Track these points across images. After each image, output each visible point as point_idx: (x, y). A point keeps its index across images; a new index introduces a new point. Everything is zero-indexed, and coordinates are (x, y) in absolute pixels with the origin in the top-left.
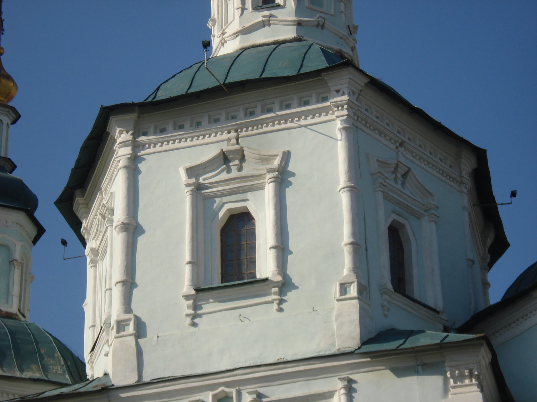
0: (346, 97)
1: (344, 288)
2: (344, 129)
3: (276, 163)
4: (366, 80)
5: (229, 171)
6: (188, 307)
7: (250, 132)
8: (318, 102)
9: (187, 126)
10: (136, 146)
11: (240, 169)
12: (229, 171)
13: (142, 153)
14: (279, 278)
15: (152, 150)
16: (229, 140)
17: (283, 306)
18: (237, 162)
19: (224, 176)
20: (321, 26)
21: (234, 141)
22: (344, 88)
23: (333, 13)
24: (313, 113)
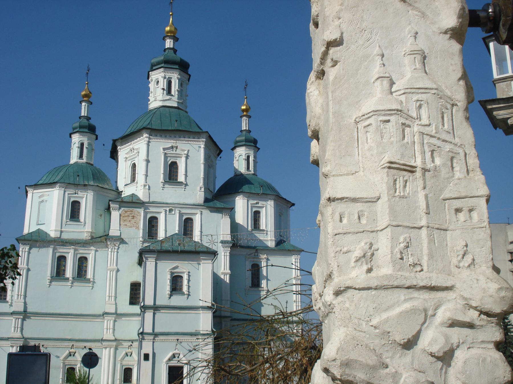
0: (205, 140)
1: (201, 188)
2: (204, 148)
3: (186, 152)
4: (208, 135)
5: (173, 151)
6: (162, 185)
8: (197, 139)
10: (150, 138)
11: (176, 151)
12: (173, 151)
13: (150, 140)
14: (186, 183)
15: (153, 140)
17: (185, 189)
18: (175, 149)
19: (172, 152)
20: (182, 103)
21: (175, 143)
24: (196, 141)
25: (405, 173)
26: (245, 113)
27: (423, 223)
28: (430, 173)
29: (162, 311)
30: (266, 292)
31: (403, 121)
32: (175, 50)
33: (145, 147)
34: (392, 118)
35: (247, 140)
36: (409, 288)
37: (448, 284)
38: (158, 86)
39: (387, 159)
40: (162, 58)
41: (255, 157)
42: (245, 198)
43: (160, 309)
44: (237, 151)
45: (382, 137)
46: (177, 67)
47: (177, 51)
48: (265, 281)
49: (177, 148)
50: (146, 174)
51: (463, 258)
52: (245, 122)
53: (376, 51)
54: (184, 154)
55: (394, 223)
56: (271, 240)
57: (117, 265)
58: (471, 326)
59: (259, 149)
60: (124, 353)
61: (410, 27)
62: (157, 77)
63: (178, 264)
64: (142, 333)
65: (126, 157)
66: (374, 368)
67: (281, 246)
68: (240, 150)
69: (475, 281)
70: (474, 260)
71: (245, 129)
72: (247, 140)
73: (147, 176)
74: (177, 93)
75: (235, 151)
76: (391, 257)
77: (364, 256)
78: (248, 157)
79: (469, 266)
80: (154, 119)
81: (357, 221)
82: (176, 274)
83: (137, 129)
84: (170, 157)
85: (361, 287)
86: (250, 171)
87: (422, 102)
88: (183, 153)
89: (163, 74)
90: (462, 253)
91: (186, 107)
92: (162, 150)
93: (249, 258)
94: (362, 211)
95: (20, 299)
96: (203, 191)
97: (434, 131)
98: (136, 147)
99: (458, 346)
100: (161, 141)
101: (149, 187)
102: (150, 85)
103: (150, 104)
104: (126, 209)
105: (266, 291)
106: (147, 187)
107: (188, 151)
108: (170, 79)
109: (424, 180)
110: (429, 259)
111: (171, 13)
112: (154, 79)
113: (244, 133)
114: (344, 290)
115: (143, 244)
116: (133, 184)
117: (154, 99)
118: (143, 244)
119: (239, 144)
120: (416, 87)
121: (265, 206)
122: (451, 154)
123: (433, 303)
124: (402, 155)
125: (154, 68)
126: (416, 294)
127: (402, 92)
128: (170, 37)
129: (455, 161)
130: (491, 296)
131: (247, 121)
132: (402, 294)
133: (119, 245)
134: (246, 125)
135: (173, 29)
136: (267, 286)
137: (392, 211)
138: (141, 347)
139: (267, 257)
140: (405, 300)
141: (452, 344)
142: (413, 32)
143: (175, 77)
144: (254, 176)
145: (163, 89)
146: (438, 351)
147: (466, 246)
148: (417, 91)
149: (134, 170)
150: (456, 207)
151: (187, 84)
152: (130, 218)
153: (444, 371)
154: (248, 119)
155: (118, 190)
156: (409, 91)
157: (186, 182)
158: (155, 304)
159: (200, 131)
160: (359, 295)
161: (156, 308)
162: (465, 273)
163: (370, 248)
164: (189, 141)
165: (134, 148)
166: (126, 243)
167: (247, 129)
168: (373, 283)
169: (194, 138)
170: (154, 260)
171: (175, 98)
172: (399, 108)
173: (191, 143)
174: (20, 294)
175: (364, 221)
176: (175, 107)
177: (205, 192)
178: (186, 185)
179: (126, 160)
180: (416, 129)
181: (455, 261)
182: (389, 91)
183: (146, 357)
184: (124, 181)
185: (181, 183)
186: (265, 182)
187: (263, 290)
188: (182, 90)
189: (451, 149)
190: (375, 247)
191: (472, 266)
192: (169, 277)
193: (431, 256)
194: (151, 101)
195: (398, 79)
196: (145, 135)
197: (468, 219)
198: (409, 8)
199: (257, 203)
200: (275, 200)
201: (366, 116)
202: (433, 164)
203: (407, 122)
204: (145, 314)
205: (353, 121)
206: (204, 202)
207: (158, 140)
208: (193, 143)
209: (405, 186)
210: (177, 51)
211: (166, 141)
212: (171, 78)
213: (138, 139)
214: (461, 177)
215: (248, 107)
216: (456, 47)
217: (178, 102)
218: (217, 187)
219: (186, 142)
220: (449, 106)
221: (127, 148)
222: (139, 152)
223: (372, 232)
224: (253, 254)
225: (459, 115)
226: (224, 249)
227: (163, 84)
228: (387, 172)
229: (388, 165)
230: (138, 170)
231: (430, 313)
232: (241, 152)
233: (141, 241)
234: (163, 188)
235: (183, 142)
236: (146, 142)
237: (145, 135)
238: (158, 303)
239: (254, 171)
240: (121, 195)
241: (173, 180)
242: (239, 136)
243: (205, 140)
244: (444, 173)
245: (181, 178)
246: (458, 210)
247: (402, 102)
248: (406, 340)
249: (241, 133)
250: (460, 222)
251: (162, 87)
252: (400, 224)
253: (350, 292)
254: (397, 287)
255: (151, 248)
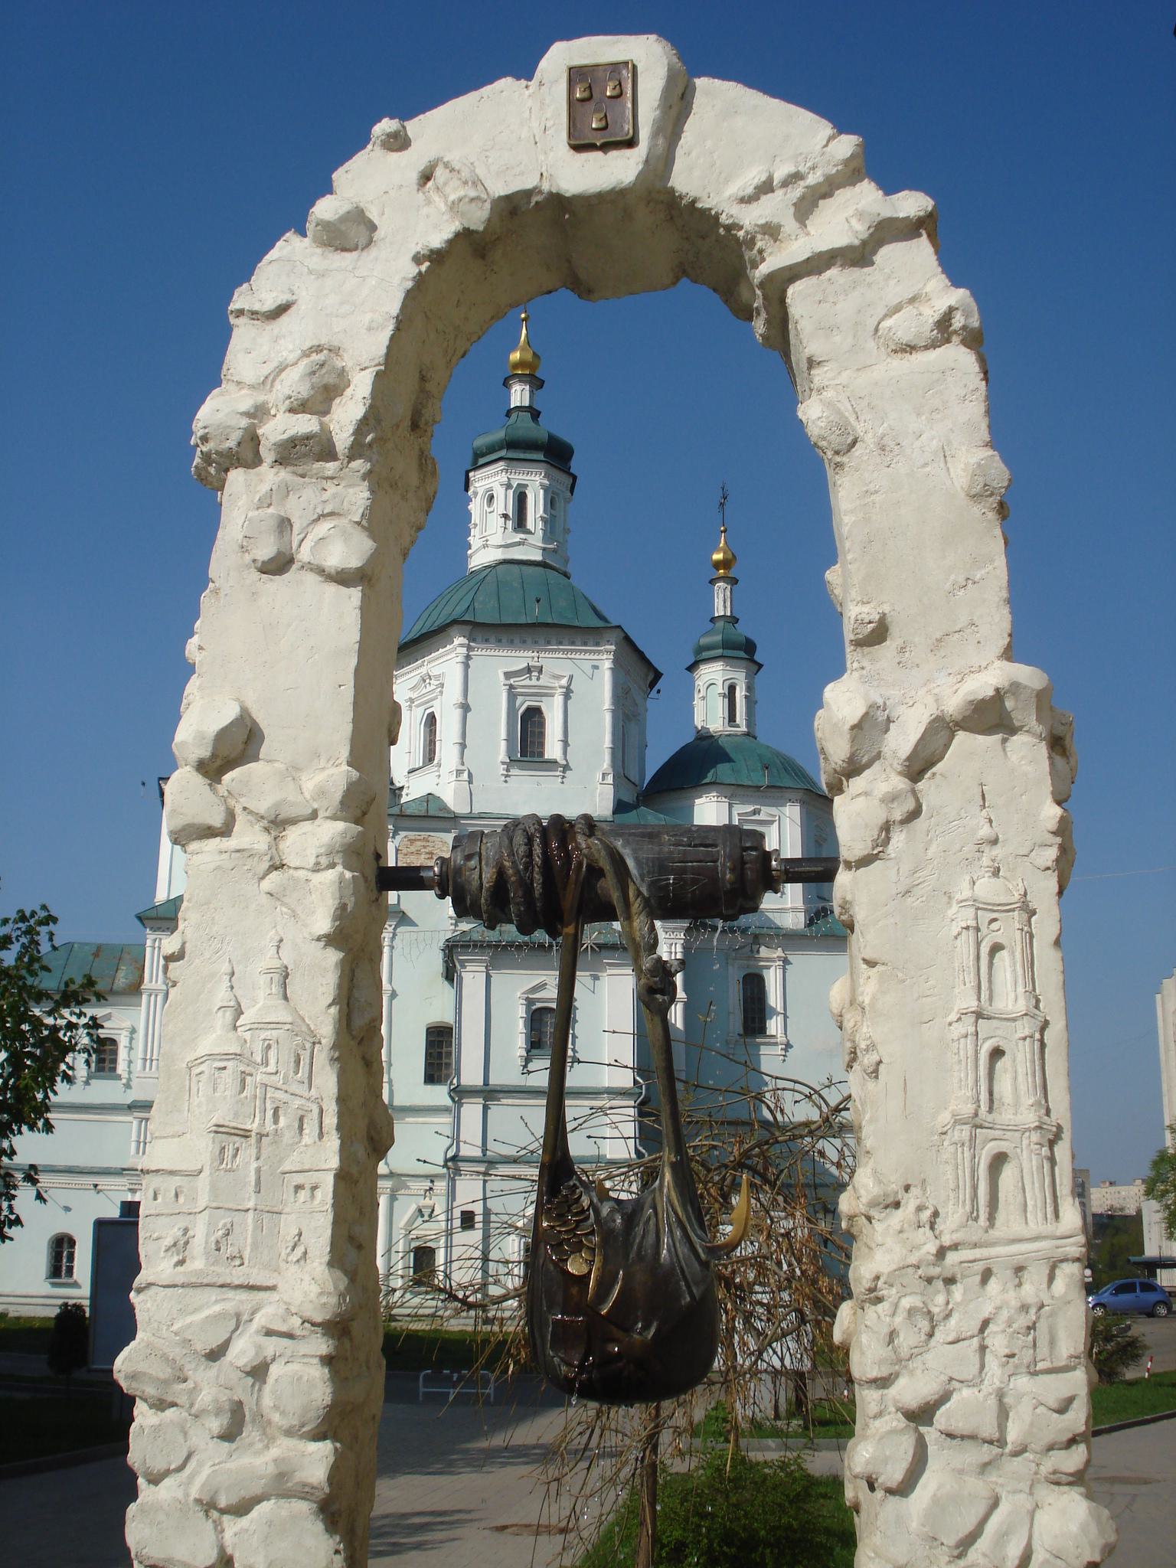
0: (613, 647)
3: (564, 682)
4: (623, 635)
5: (531, 679)
7: (546, 655)
8: (594, 646)
9: (504, 640)
10: (469, 648)
11: (538, 679)
12: (531, 679)
14: (564, 763)
15: (479, 653)
16: (533, 658)
18: (536, 674)
19: (527, 682)
20: (555, 551)
21: (536, 659)
22: (613, 639)
23: (561, 541)
24: (590, 652)
25: (237, 1138)
26: (722, 571)
27: (251, 1204)
28: (268, 1138)
29: (504, 1101)
30: (782, 1049)
31: (242, 1068)
32: (534, 413)
33: (458, 670)
34: (230, 1064)
35: (727, 644)
36: (222, 1286)
37: (270, 1283)
38: (491, 509)
39: (214, 1121)
40: (500, 435)
41: (749, 688)
42: (724, 799)
43: (501, 1095)
44: (702, 672)
45: (215, 1090)
46: (540, 456)
47: (539, 413)
48: (779, 1018)
49: (540, 670)
50: (461, 741)
51: (293, 1250)
52: (721, 596)
53: (225, 968)
54: (561, 687)
55: (214, 1205)
56: (794, 909)
57: (391, 983)
58: (290, 1336)
59: (760, 666)
60: (414, 1207)
61: (274, 931)
62: (487, 487)
63: (544, 978)
64: (455, 1158)
65: (410, 698)
66: (166, 1383)
67: (822, 926)
68: (710, 670)
69: (299, 1281)
70: (305, 1253)
71: (722, 614)
72: (727, 644)
73: (463, 746)
74: (540, 525)
75: (696, 675)
76: (205, 1248)
77: (175, 1245)
78: (732, 689)
79: (298, 1261)
80: (480, 598)
81: (174, 1199)
82: (539, 1005)
83: (436, 624)
84: (522, 694)
85: (164, 1284)
86: (738, 726)
87: (271, 1042)
88: (557, 685)
89: (503, 477)
90: (291, 1244)
91: (567, 561)
92: (502, 677)
93: (735, 959)
94: (180, 1187)
95: (151, 1069)
96: (611, 782)
97: (281, 1082)
98: (434, 672)
99: (273, 1360)
100: (501, 653)
101: (470, 775)
102: (471, 506)
103: (471, 556)
104: (412, 835)
105: (784, 1046)
106: (465, 776)
107: (571, 678)
108: (522, 490)
109: (259, 1149)
110: (252, 1251)
111: (523, 316)
112: (481, 492)
113: (720, 624)
114: (145, 1287)
115: (456, 925)
116: (431, 768)
117: (480, 543)
118: (456, 925)
119: (706, 654)
120: (264, 1021)
121: (777, 818)
122: (301, 1113)
123: (250, 1306)
124: (236, 1115)
125: (481, 461)
126: (231, 1294)
127: (248, 1027)
128: (521, 379)
129: (306, 1120)
130: (311, 1302)
131: (728, 593)
132: (214, 1294)
133: (395, 929)
134: (725, 602)
135: (529, 356)
136: (786, 1034)
137: (214, 1190)
138: (452, 1194)
139: (783, 955)
140: (217, 1302)
141: (265, 1357)
142: (277, 938)
143: (535, 482)
144: (748, 740)
145: (505, 516)
146: (244, 1366)
147: (300, 1235)
148: (265, 1026)
149: (431, 730)
150: (295, 1184)
151: (567, 501)
152: (423, 856)
153: (257, 1388)
154: (729, 587)
155: (392, 783)
156: (256, 1026)
157: (567, 761)
158: (486, 1083)
159: (601, 624)
160: (163, 1293)
161: (489, 1094)
162: (294, 1268)
163: (185, 1234)
164: (572, 651)
165: (431, 674)
166: (412, 923)
167: (729, 614)
168: (180, 1280)
169: (585, 644)
170: (484, 969)
171: (537, 539)
172: (238, 1052)
173: (577, 656)
174: (148, 1057)
175: (181, 1199)
176: (535, 561)
177: (616, 785)
178: (566, 767)
179: (410, 706)
180: (259, 1078)
181: (283, 1255)
182: (231, 1026)
183: (468, 1220)
184: (407, 760)
185: (554, 763)
186: (778, 754)
187: (776, 1044)
188: (553, 517)
189: (302, 1105)
190: (191, 1233)
191: (302, 1262)
192: (521, 1011)
193: (255, 1246)
194: (474, 548)
195: (249, 1007)
196: (459, 640)
197: (309, 1200)
198: (278, 903)
199: (755, 812)
200: (803, 803)
201: (199, 1061)
202: (274, 1126)
203: (248, 1070)
204: (462, 1109)
205: (185, 1066)
206: (614, 813)
207: (492, 653)
208: (582, 656)
209: (235, 1156)
210: (539, 413)
211: (513, 654)
212: (527, 485)
213: (441, 650)
214: (309, 1143)
215: (730, 556)
216: (333, 956)
217: (544, 549)
218: (651, 771)
219: (564, 656)
220: (308, 1045)
221: (412, 674)
222: (442, 685)
223: (190, 1214)
224: (748, 949)
225: (322, 1056)
226: (667, 936)
227: (504, 502)
228: (213, 1138)
229: (214, 1128)
230: (441, 732)
231: (245, 1317)
232: (713, 675)
233: (451, 918)
234: (507, 776)
235: (556, 656)
236: (460, 659)
237: (459, 640)
238: (494, 1080)
239: (748, 726)
240: (400, 796)
241: (533, 754)
242: (707, 633)
243: (613, 647)
244: (288, 1137)
245: (553, 750)
246: (298, 1188)
247: (245, 1041)
248: (208, 1351)
249: (712, 625)
250: (297, 1204)
251: (502, 511)
252: (221, 1205)
253: (154, 1289)
254: (207, 1285)
255: (476, 937)
